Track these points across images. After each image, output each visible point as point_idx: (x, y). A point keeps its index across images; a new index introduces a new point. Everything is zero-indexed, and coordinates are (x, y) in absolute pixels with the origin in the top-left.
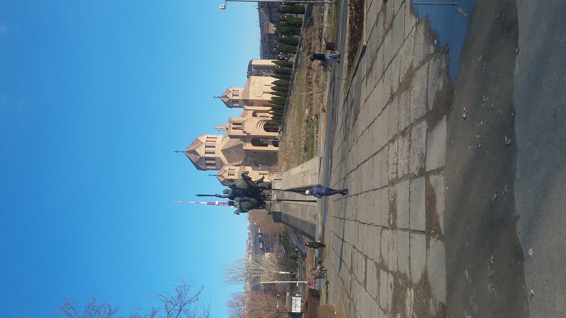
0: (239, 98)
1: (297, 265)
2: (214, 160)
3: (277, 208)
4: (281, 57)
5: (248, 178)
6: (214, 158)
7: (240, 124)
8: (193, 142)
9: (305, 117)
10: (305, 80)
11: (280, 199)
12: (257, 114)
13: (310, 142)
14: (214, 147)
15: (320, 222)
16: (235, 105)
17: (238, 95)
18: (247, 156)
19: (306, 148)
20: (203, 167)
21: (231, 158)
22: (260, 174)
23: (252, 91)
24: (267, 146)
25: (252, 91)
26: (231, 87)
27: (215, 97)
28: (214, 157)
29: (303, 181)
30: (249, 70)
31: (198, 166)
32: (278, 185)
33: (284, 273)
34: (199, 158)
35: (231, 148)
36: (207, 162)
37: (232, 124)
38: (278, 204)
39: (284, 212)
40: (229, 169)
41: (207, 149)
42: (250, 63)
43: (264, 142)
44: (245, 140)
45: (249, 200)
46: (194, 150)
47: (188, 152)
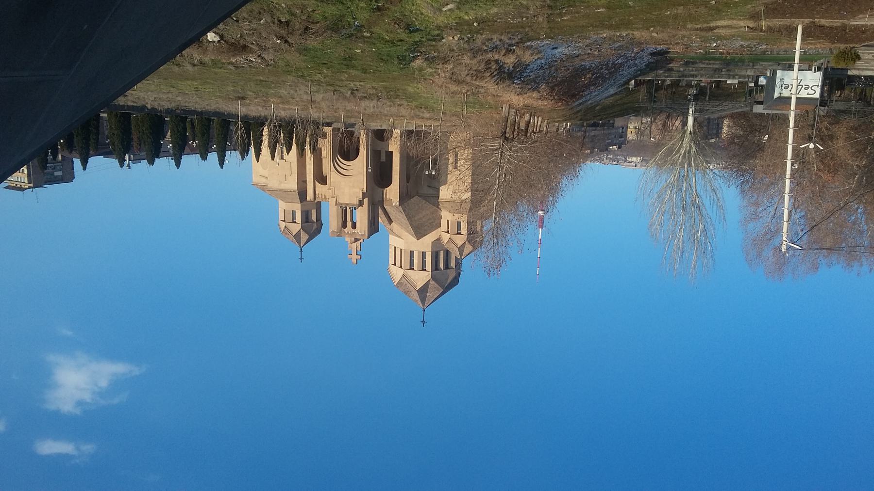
0: (297, 208)
1: (675, 84)
6: (435, 254)
8: (404, 293)
14: (412, 253)
18: (417, 194)
20: (452, 274)
21: (432, 220)
23: (281, 182)
24: (392, 152)
25: (281, 182)
26: (278, 224)
31: (450, 284)
36: (441, 266)
37: (346, 230)
40: (448, 232)
41: (415, 267)
44: (379, 201)
46: (417, 291)
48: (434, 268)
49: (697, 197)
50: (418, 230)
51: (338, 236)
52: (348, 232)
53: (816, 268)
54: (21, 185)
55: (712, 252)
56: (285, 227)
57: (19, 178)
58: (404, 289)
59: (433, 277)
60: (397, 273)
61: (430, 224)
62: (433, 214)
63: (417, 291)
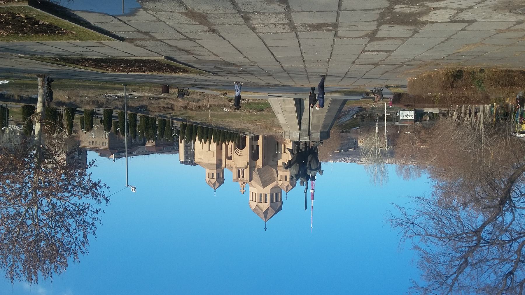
2: (272, 194)
3: (316, 135)
5: (289, 164)
6: (271, 195)
7: (239, 171)
10: (197, 112)
11: (308, 133)
12: (229, 156)
14: (260, 195)
15: (329, 95)
17: (213, 174)
20: (279, 205)
22: (285, 152)
23: (209, 161)
25: (209, 161)
27: (215, 195)
29: (291, 112)
30: (189, 164)
31: (278, 209)
32: (295, 135)
33: (377, 128)
36: (274, 200)
37: (240, 179)
38: (313, 134)
39: (319, 130)
40: (281, 180)
42: (182, 163)
43: (255, 148)
45: (310, 162)
46: (264, 213)
47: (266, 218)
48: (271, 202)
53: (420, 175)
63: (264, 213)
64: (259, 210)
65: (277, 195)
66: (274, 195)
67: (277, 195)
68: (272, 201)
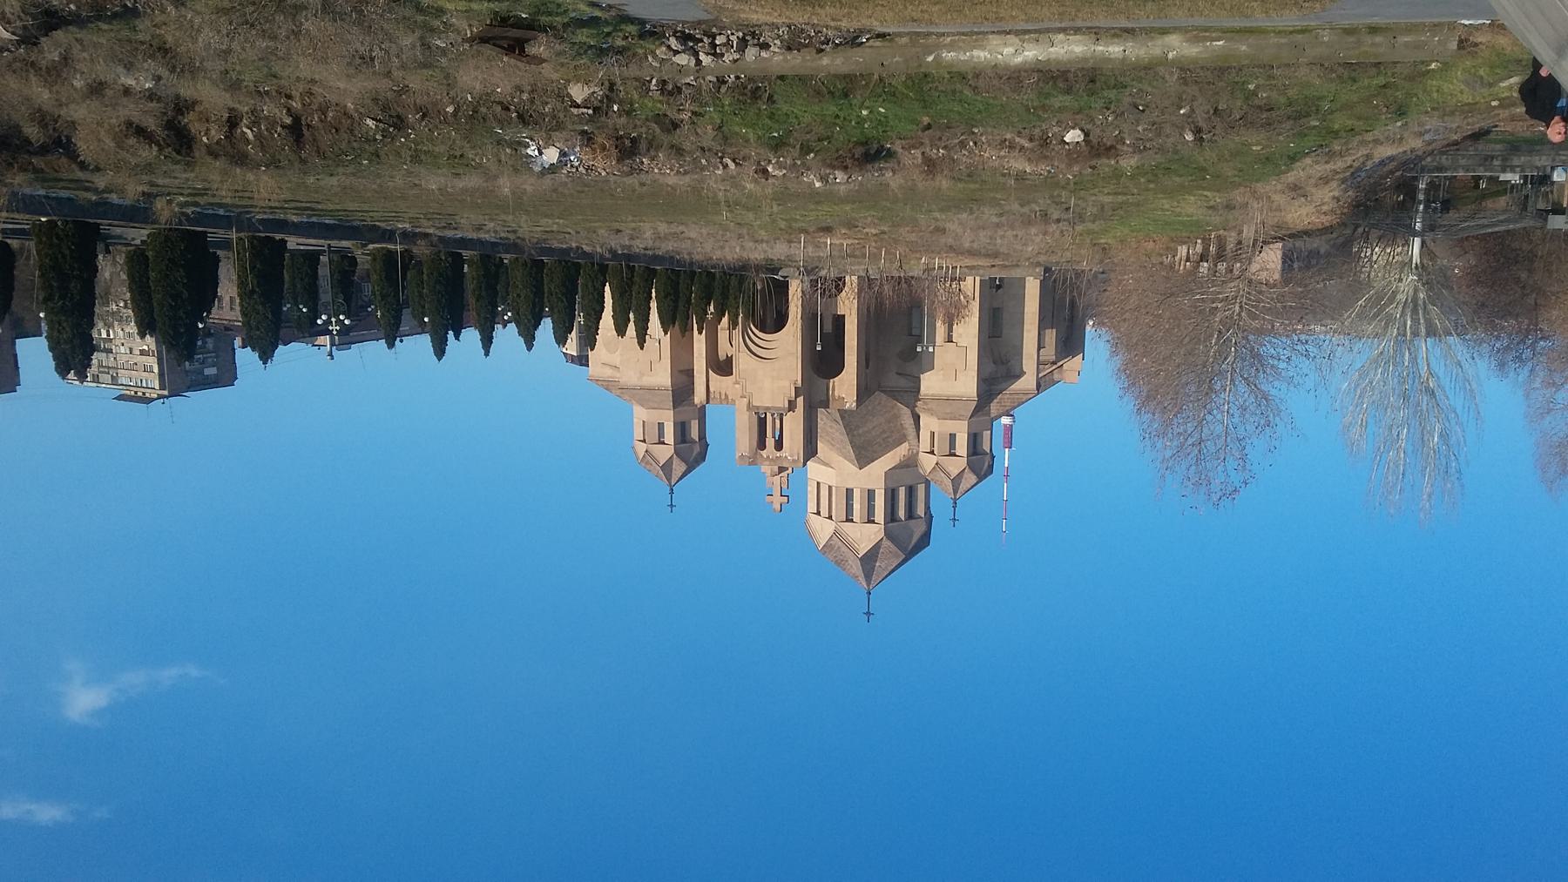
0: (668, 419)
4: (341, 317)
7: (762, 423)
9: (604, 166)
12: (722, 356)
13: (803, 112)
14: (849, 492)
16: (695, 434)
17: (661, 426)
19: (859, 151)
20: (918, 529)
21: (888, 434)
22: (950, 340)
23: (642, 375)
28: (883, 491)
34: (889, 543)
35: (854, 436)
36: (902, 513)
37: (764, 453)
40: (932, 452)
41: (856, 516)
43: (829, 328)
44: (821, 401)
46: (861, 559)
47: (868, 577)
48: (889, 519)
49: (1430, 376)
50: (863, 452)
51: (750, 464)
52: (768, 457)
54: (144, 394)
55: (1459, 472)
56: (647, 451)
57: (144, 381)
58: (836, 557)
59: (888, 534)
60: (823, 529)
61: (883, 440)
62: (889, 422)
63: (861, 559)
64: (844, 549)
65: (911, 492)
66: (902, 493)
67: (911, 492)
68: (891, 515)
